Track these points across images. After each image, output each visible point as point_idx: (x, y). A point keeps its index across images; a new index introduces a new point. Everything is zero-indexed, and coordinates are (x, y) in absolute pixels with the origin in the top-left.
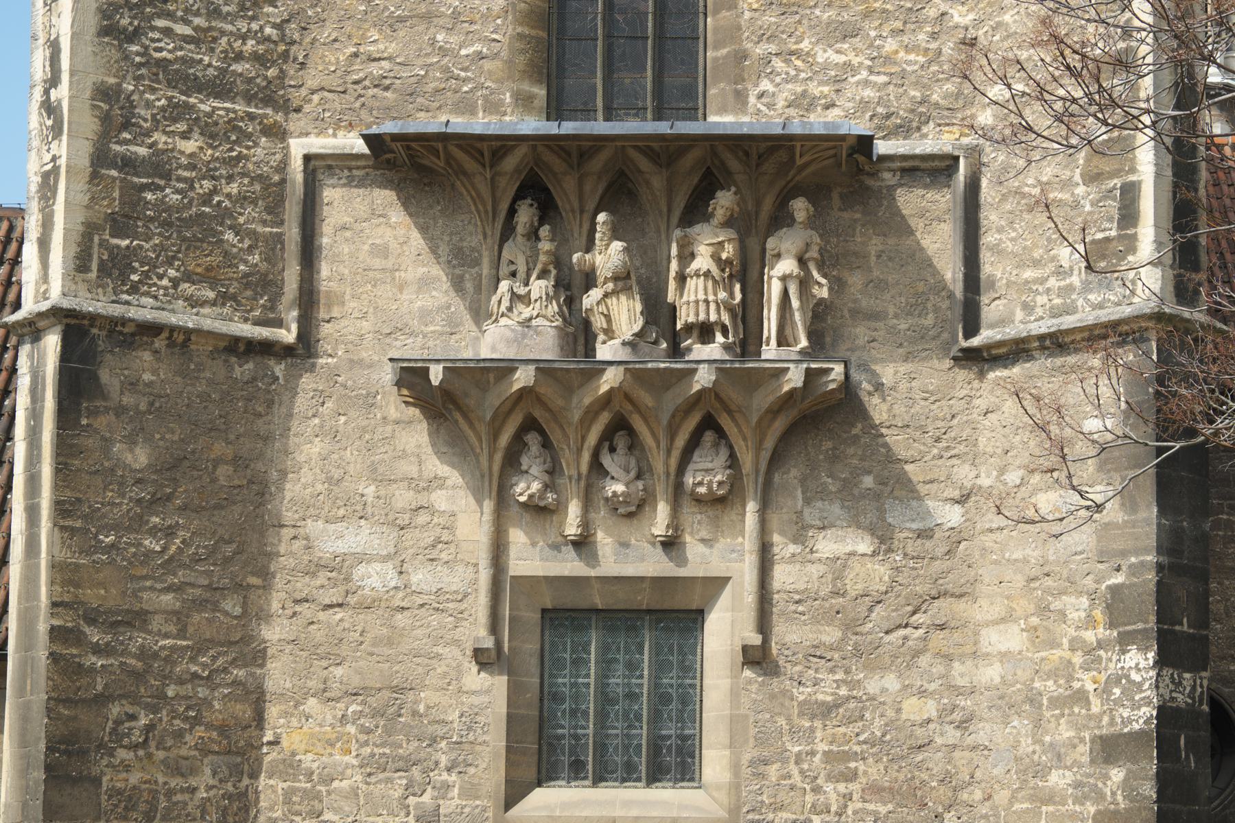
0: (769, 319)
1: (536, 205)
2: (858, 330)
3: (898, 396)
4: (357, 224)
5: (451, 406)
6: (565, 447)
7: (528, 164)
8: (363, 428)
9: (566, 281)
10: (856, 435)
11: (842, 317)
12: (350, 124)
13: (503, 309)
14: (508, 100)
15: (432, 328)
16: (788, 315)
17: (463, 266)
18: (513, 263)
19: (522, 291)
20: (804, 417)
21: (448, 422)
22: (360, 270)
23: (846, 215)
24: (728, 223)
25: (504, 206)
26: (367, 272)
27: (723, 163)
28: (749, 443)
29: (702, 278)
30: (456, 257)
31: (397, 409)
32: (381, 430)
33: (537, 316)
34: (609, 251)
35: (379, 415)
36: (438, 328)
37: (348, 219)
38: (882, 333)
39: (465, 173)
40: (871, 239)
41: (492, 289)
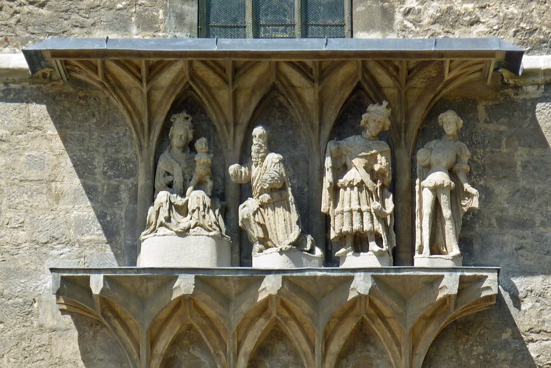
0: (421, 229)
1: (190, 119)
2: (506, 238)
3: (546, 302)
4: (14, 136)
5: (110, 314)
6: (221, 353)
7: (183, 79)
8: (21, 335)
9: (220, 191)
10: (507, 342)
11: (490, 225)
12: (6, 40)
13: (162, 218)
14: (161, 17)
15: (88, 237)
16: (439, 224)
17: (118, 177)
18: (169, 174)
19: (179, 201)
20: (455, 322)
21: (104, 330)
22: (16, 181)
23: (492, 127)
24: (381, 136)
25: (160, 119)
26: (22, 184)
27: (373, 78)
28: (403, 349)
29: (356, 188)
30: (111, 168)
31: (53, 317)
32: (38, 337)
33: (195, 226)
34: (265, 164)
35: (35, 324)
36: (93, 237)
37: (4, 132)
38: (529, 240)
39: (121, 88)
40: (516, 150)
41: (148, 199)
